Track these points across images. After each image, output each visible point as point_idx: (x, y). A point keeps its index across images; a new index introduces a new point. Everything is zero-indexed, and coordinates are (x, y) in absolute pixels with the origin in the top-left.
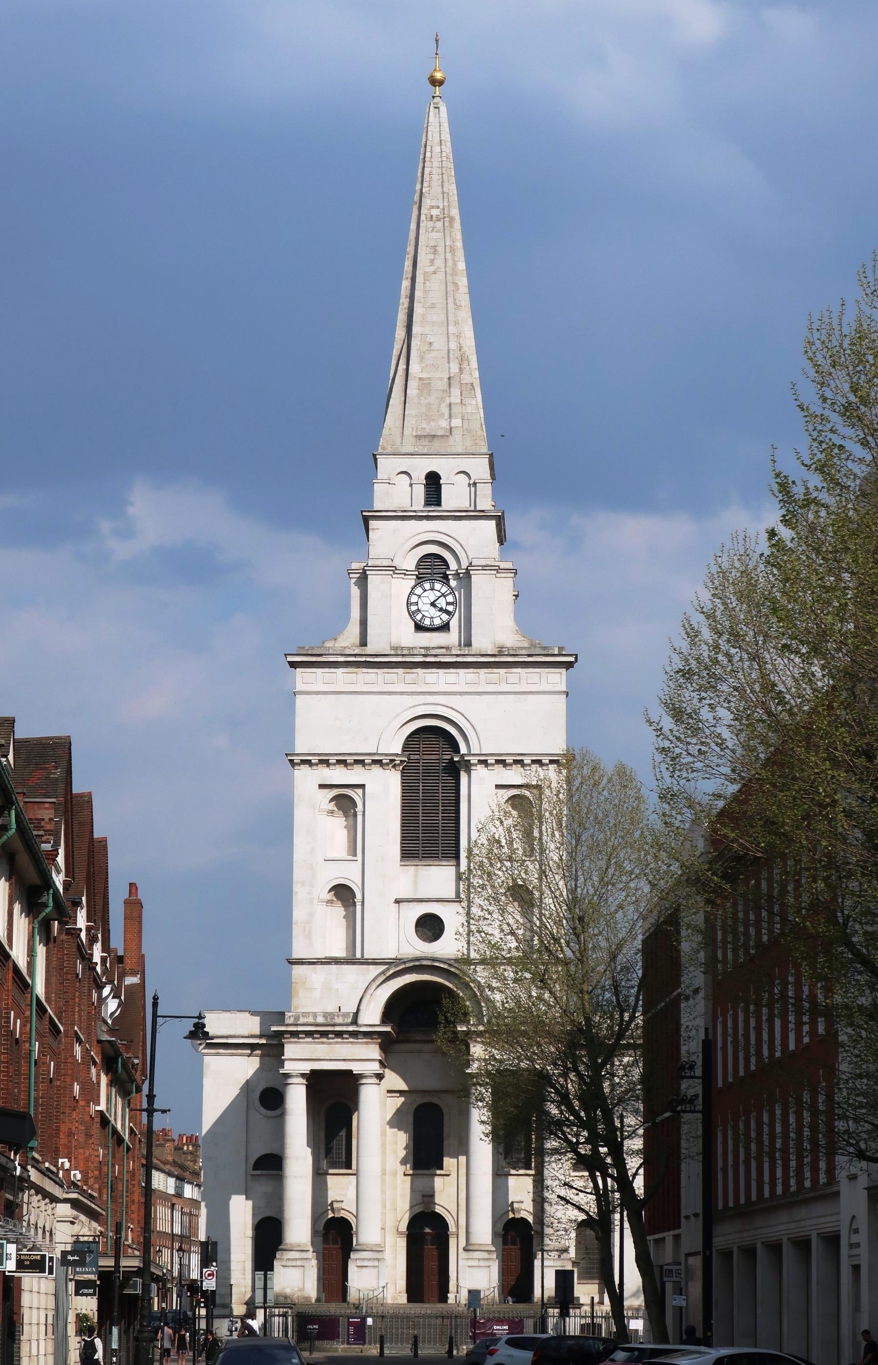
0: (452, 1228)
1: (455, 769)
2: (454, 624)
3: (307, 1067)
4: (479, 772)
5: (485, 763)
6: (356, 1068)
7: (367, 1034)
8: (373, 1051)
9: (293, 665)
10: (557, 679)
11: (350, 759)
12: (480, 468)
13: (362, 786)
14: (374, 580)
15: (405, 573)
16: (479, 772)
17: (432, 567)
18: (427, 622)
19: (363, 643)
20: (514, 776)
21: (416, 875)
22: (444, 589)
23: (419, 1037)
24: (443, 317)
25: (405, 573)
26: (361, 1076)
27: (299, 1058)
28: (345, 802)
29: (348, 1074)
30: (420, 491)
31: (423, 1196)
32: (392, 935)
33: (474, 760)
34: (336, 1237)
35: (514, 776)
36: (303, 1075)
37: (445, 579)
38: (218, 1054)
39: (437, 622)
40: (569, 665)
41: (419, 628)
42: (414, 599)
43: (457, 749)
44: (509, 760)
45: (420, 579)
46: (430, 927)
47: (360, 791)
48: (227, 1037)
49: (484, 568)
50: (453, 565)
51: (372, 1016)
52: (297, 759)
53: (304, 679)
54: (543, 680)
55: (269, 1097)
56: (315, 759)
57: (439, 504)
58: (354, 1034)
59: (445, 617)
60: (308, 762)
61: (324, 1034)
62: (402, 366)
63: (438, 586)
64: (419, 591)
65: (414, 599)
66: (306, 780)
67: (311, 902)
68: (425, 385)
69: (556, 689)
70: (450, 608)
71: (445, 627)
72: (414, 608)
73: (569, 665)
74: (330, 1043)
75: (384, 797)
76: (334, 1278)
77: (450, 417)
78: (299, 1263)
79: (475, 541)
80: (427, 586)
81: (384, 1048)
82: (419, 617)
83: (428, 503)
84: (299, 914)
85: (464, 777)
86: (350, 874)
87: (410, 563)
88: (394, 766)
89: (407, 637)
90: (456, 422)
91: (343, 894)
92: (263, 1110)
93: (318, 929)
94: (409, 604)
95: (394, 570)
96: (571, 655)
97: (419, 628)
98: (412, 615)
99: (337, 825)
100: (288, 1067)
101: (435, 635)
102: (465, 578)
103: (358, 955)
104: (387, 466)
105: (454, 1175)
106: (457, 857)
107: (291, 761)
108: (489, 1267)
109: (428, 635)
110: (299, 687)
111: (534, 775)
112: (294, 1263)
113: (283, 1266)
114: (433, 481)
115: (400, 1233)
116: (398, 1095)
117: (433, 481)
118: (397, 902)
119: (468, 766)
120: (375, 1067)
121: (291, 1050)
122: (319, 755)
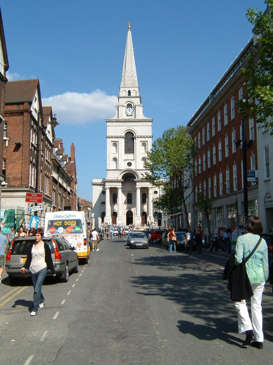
0: (133, 213)
1: (133, 139)
2: (133, 115)
3: (109, 187)
6: (118, 187)
8: (120, 184)
9: (107, 122)
10: (150, 124)
12: (137, 90)
13: (118, 141)
14: (120, 108)
15: (125, 107)
16: (137, 139)
17: (129, 106)
18: (128, 115)
19: (118, 118)
20: (143, 139)
21: (127, 156)
22: (132, 109)
23: (128, 182)
24: (131, 65)
25: (125, 107)
26: (119, 188)
27: (108, 185)
28: (115, 144)
29: (116, 188)
30: (127, 93)
32: (123, 166)
33: (137, 137)
34: (114, 215)
35: (143, 139)
37: (131, 108)
39: (130, 115)
40: (152, 121)
41: (127, 115)
42: (126, 111)
43: (133, 135)
44: (142, 137)
45: (127, 107)
46: (129, 164)
49: (138, 105)
50: (133, 105)
51: (120, 178)
52: (107, 137)
53: (108, 124)
55: (104, 192)
56: (110, 137)
57: (130, 95)
59: (132, 114)
62: (124, 73)
63: (130, 109)
65: (126, 111)
66: (109, 141)
68: (128, 76)
69: (150, 125)
70: (132, 112)
71: (132, 115)
72: (126, 112)
73: (152, 121)
75: (122, 143)
76: (114, 221)
79: (137, 101)
80: (129, 109)
82: (127, 114)
83: (128, 95)
84: (108, 162)
85: (135, 140)
86: (116, 156)
87: (126, 105)
88: (123, 138)
89: (125, 117)
91: (115, 159)
92: (102, 194)
93: (111, 165)
94: (126, 112)
95: (123, 106)
97: (127, 115)
98: (126, 113)
99: (114, 148)
100: (106, 187)
101: (130, 116)
102: (135, 108)
103: (118, 169)
104: (122, 89)
106: (134, 153)
107: (106, 137)
109: (128, 117)
110: (108, 125)
111: (147, 139)
114: (129, 92)
117: (129, 92)
118: (124, 160)
119: (135, 138)
120: (121, 187)
121: (107, 184)
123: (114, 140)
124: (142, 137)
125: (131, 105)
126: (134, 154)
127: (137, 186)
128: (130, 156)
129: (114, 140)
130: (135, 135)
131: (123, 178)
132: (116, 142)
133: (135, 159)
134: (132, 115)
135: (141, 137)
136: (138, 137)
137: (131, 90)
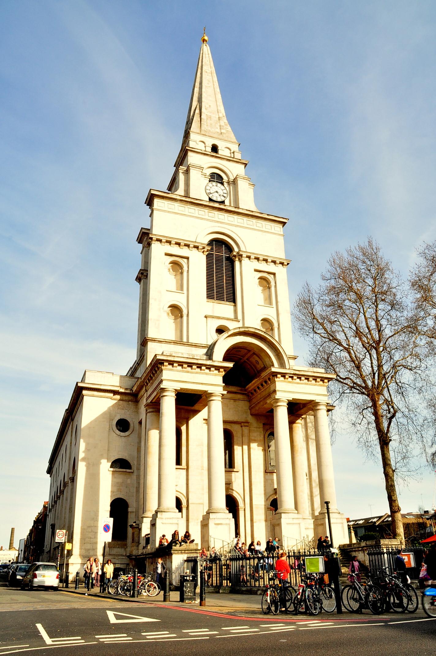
1: (231, 261)
5: (249, 257)
6: (210, 389)
7: (218, 368)
10: (278, 228)
13: (188, 258)
16: (245, 261)
18: (214, 199)
33: (244, 255)
37: (222, 184)
38: (93, 396)
44: (261, 258)
47: (186, 260)
54: (273, 228)
58: (209, 367)
60: (160, 241)
61: (190, 365)
63: (219, 185)
68: (209, 118)
70: (225, 195)
72: (208, 191)
73: (284, 224)
77: (220, 129)
80: (214, 184)
81: (226, 380)
85: (237, 264)
86: (180, 300)
90: (223, 131)
91: (175, 309)
92: (118, 432)
94: (206, 189)
98: (208, 194)
102: (234, 183)
105: (241, 472)
106: (234, 301)
108: (299, 524)
114: (215, 149)
117: (215, 149)
123: (175, 250)
125: (222, 178)
126: (235, 306)
128: (224, 309)
129: (175, 250)
130: (236, 249)
133: (240, 317)
134: (223, 202)
137: (221, 145)
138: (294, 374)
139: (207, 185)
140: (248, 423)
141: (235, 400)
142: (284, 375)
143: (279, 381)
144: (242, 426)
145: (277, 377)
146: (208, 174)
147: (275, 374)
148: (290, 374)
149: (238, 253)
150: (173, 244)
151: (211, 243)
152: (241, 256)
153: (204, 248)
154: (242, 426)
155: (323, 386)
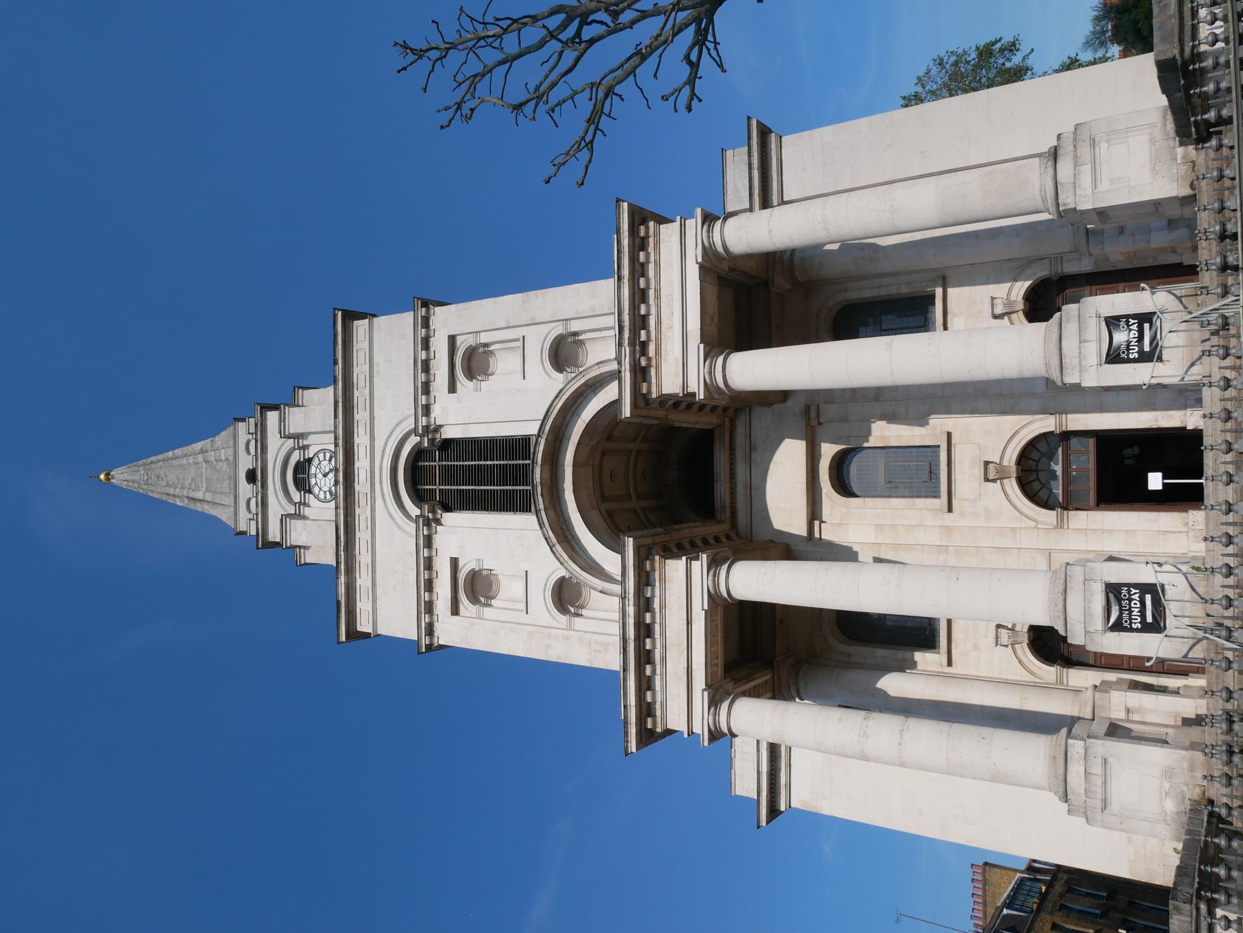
4: (438, 415)
7: (644, 579)
11: (424, 575)
22: (316, 462)
23: (721, 489)
31: (987, 480)
33: (423, 421)
36: (714, 703)
37: (310, 461)
44: (422, 377)
45: (310, 492)
48: (759, 773)
52: (425, 641)
56: (426, 619)
58: (644, 605)
63: (313, 470)
64: (316, 490)
65: (322, 496)
67: (567, 638)
72: (328, 496)
74: (664, 648)
78: (1097, 769)
80: (313, 481)
96: (335, 316)
112: (1098, 781)
113: (1104, 808)
115: (1060, 524)
116: (817, 523)
120: (699, 566)
122: (419, 613)
124: (422, 377)
127: (696, 386)
131: (618, 548)
132: (462, 576)
135: (427, 388)
136: (427, 410)
138: (632, 343)
139: (317, 497)
140: (808, 408)
141: (751, 448)
142: (641, 374)
143: (659, 386)
144: (820, 424)
145: (649, 392)
146: (296, 496)
147: (640, 399)
148: (633, 353)
149: (422, 436)
150: (431, 596)
151: (419, 497)
152: (426, 429)
153: (427, 523)
154: (820, 424)
155: (657, 234)
